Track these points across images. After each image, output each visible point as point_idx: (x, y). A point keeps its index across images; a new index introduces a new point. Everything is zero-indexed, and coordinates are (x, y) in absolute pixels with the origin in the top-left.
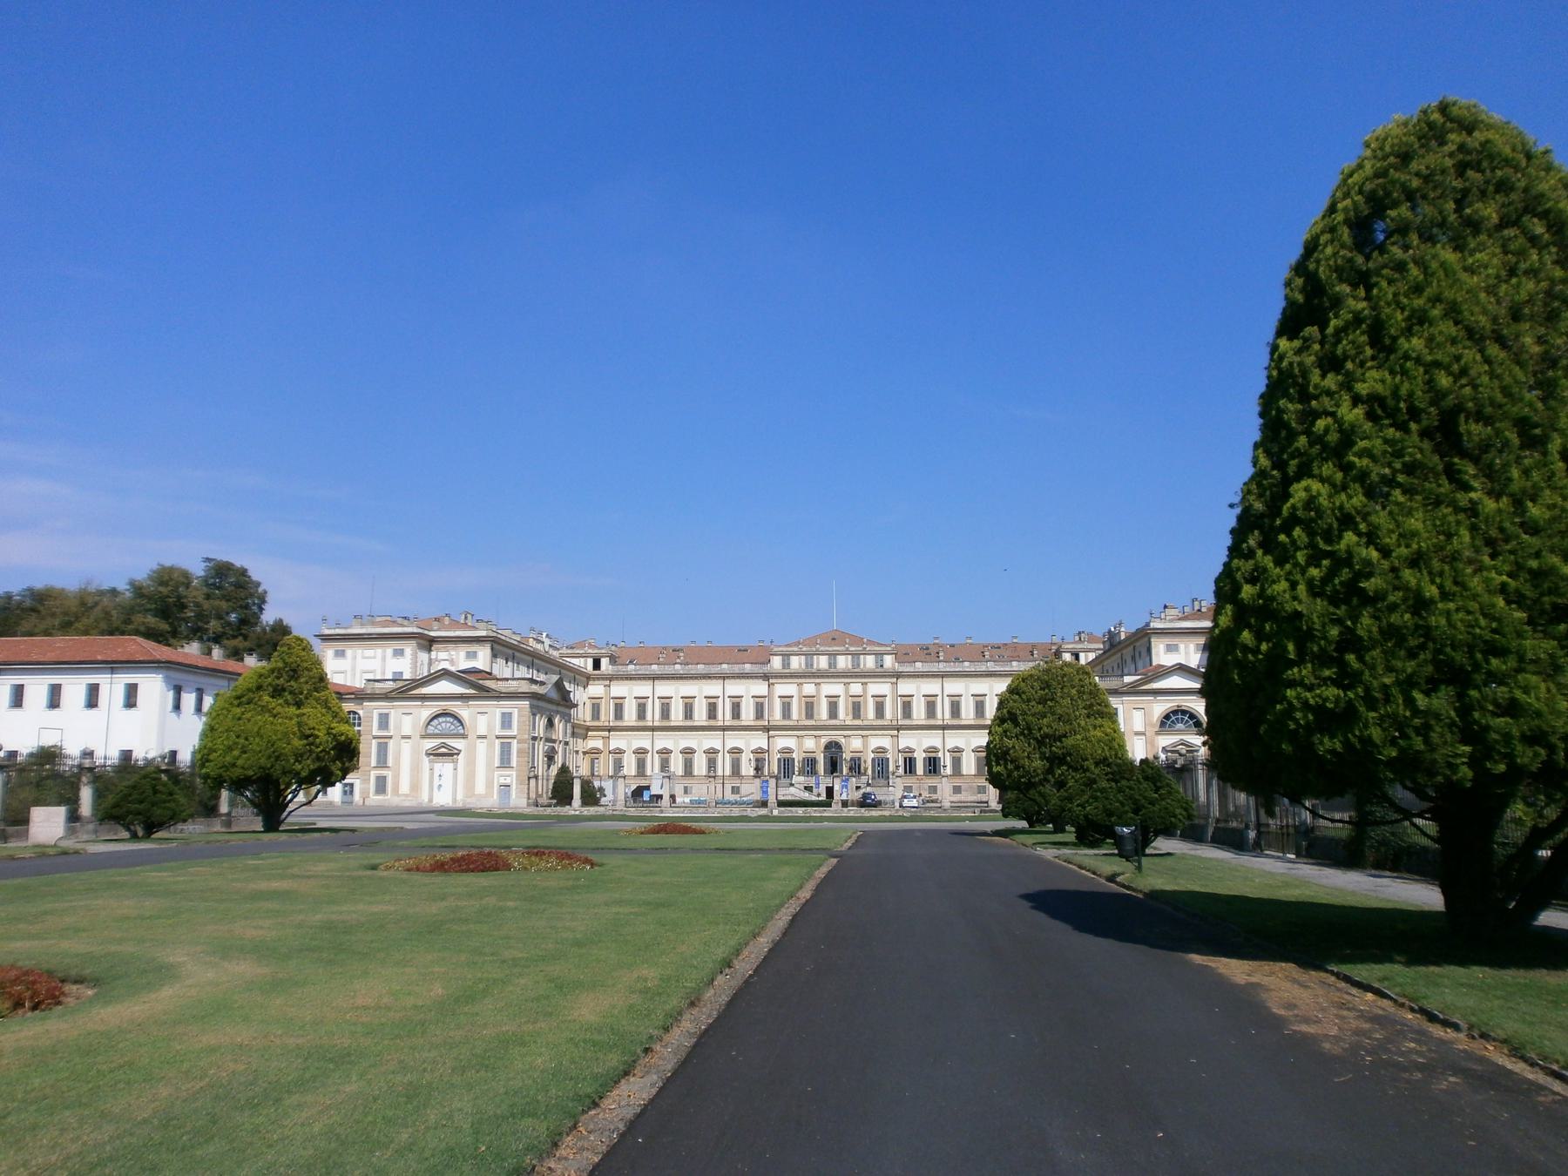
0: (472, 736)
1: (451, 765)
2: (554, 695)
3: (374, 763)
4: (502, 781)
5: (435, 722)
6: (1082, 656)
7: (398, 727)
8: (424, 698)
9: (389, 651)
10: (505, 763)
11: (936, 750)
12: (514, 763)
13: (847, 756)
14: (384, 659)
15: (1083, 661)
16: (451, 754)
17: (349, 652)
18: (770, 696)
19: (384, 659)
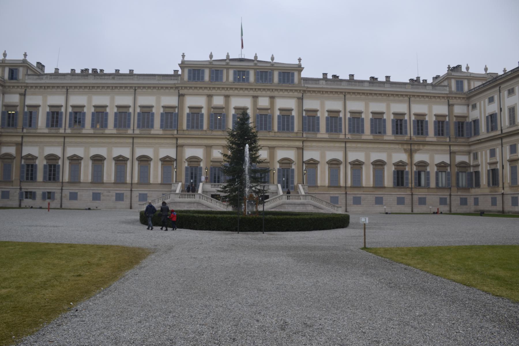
6: (466, 83)
15: (466, 88)
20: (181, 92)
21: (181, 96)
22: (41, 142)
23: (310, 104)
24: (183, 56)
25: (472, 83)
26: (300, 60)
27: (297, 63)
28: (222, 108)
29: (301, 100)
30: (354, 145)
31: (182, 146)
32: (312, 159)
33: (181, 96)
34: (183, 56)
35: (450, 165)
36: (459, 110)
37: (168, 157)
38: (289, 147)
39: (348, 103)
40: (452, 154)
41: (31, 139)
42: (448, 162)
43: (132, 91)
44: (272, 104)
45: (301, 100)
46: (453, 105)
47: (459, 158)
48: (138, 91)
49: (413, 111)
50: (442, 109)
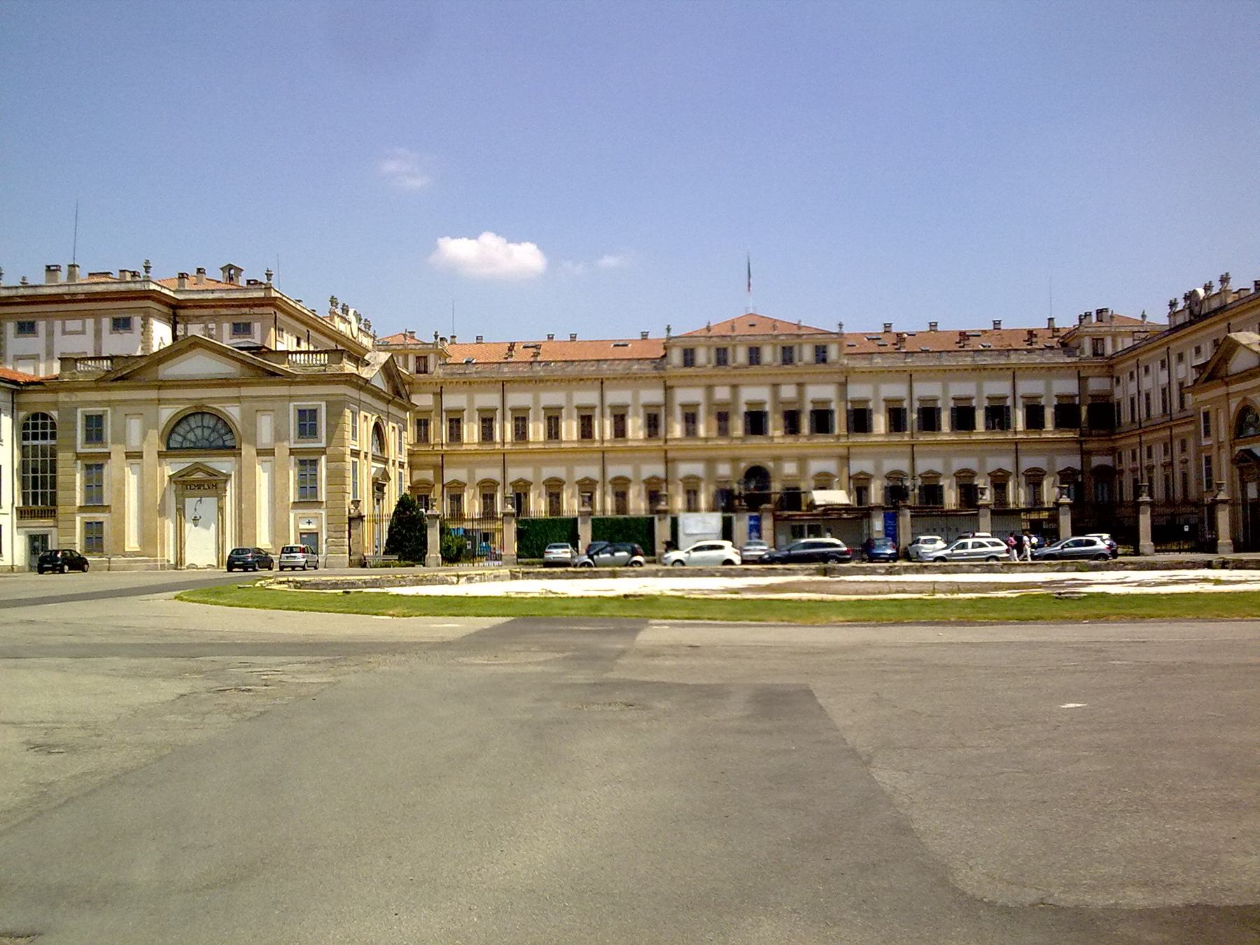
0: (248, 451)
1: (210, 503)
2: (380, 383)
3: (79, 501)
4: (304, 526)
5: (181, 430)
6: (1108, 342)
7: (121, 438)
8: (162, 385)
9: (106, 323)
10: (307, 497)
11: (937, 476)
12: (323, 497)
13: (776, 487)
14: (98, 334)
15: (1109, 350)
16: (213, 485)
17: (41, 326)
18: (668, 403)
19: (98, 334)
20: (668, 384)
21: (668, 389)
22: (470, 463)
23: (858, 391)
24: (668, 330)
25: (1119, 340)
26: (841, 325)
27: (836, 330)
28: (728, 404)
29: (843, 386)
30: (927, 449)
31: (674, 460)
32: (862, 473)
33: (668, 389)
34: (668, 330)
35: (1082, 472)
36: (1096, 385)
37: (654, 477)
38: (828, 457)
39: (915, 385)
40: (1085, 454)
41: (455, 458)
42: (1078, 467)
43: (598, 383)
44: (801, 393)
45: (843, 386)
46: (1086, 378)
47: (1096, 461)
48: (606, 383)
49: (1020, 392)
50: (1069, 386)
